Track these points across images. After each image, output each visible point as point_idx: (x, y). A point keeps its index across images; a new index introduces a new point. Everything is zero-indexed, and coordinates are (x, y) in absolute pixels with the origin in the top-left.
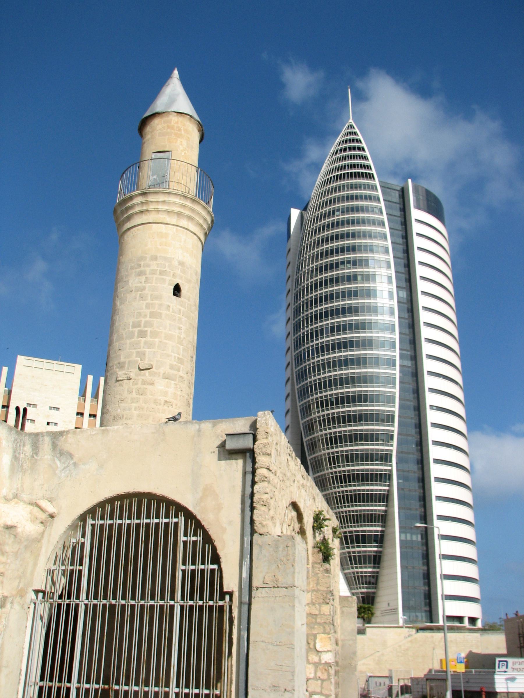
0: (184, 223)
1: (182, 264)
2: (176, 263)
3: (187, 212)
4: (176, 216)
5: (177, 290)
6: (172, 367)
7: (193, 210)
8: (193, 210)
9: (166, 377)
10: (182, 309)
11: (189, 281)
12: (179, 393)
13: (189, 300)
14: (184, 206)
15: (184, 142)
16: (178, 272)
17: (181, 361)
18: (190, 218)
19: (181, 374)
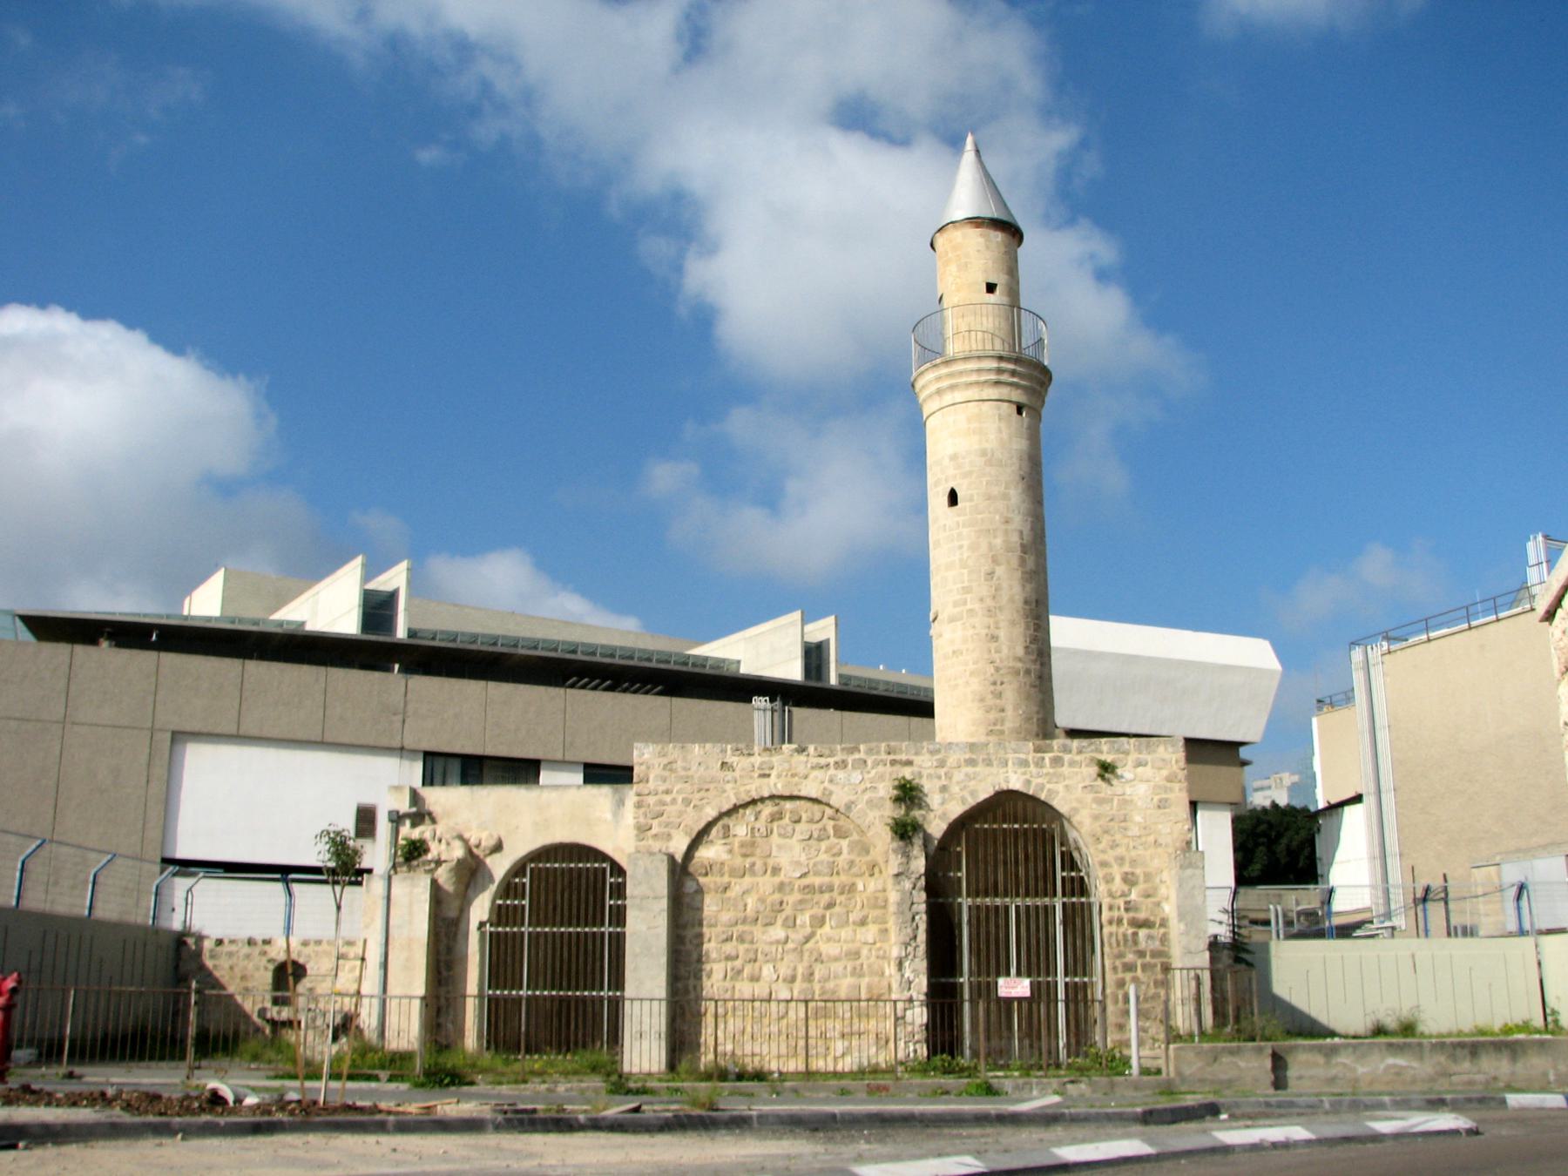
0: (948, 398)
1: (954, 457)
2: (946, 462)
3: (945, 383)
4: (937, 398)
5: (953, 498)
6: (956, 604)
7: (951, 375)
8: (951, 375)
9: (952, 620)
10: (961, 519)
11: (966, 475)
12: (971, 632)
13: (971, 500)
14: (939, 379)
15: (953, 268)
16: (951, 472)
17: (967, 590)
18: (952, 387)
19: (969, 606)
